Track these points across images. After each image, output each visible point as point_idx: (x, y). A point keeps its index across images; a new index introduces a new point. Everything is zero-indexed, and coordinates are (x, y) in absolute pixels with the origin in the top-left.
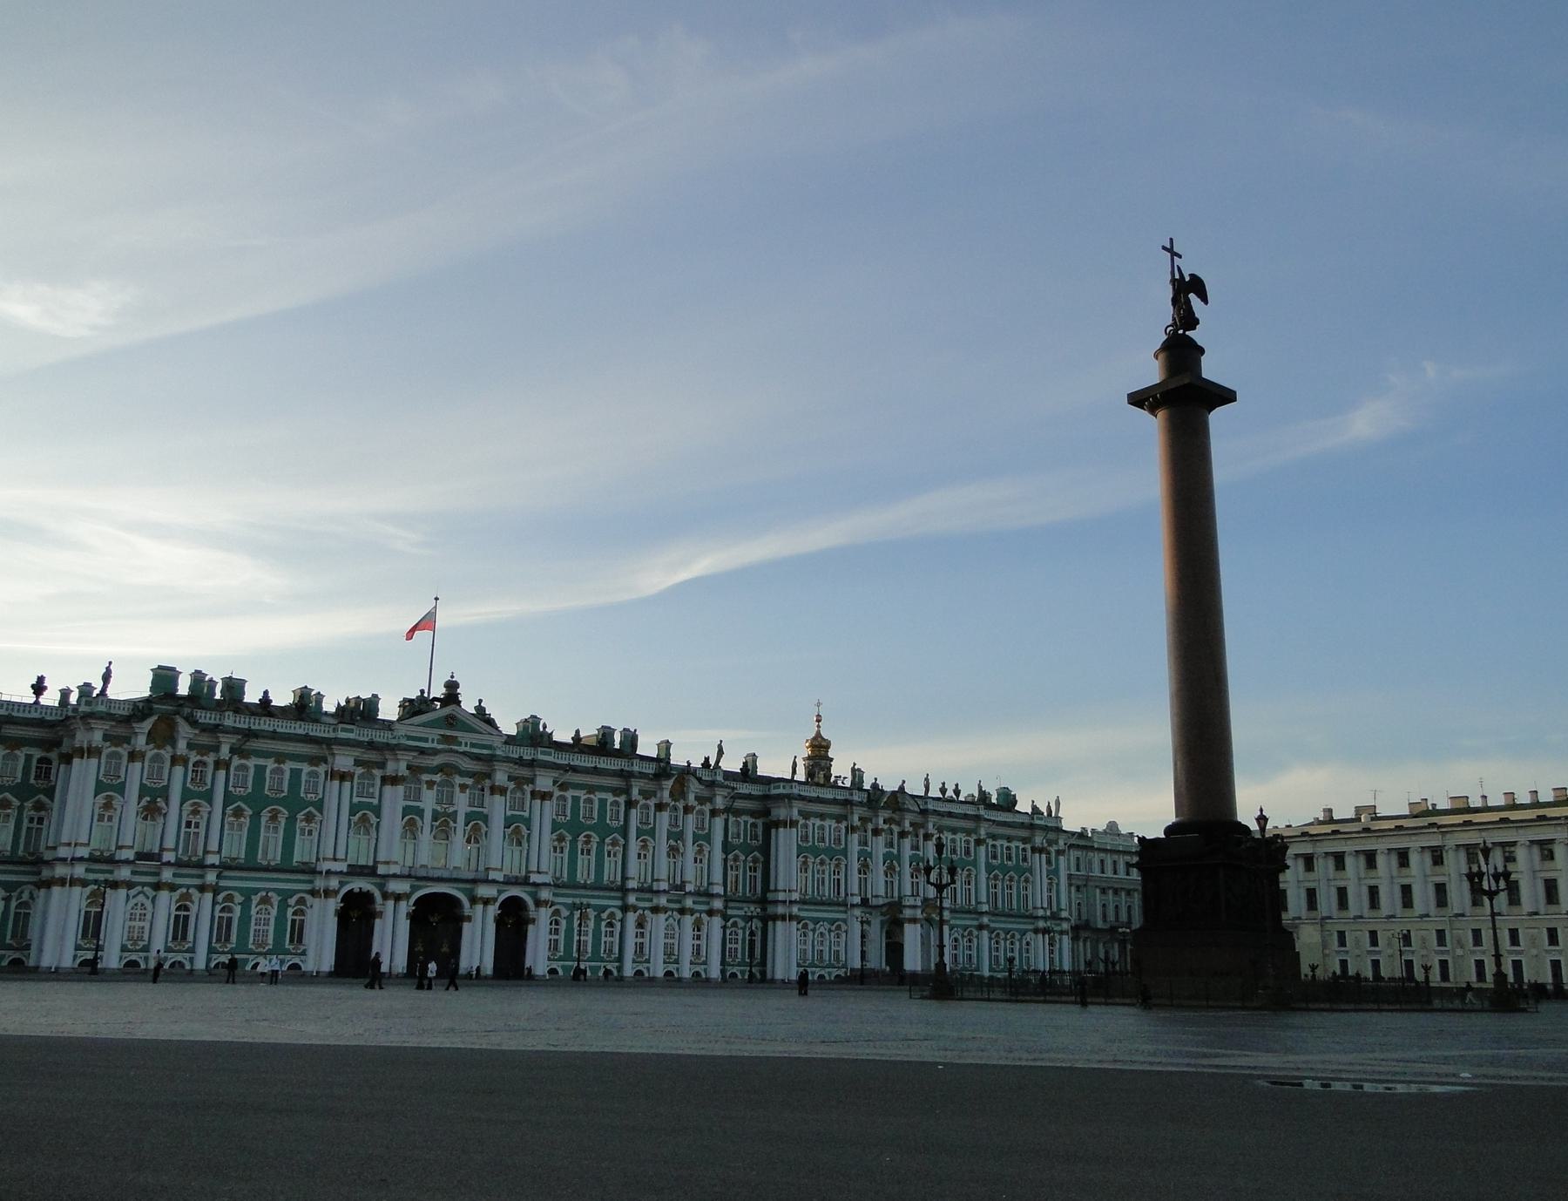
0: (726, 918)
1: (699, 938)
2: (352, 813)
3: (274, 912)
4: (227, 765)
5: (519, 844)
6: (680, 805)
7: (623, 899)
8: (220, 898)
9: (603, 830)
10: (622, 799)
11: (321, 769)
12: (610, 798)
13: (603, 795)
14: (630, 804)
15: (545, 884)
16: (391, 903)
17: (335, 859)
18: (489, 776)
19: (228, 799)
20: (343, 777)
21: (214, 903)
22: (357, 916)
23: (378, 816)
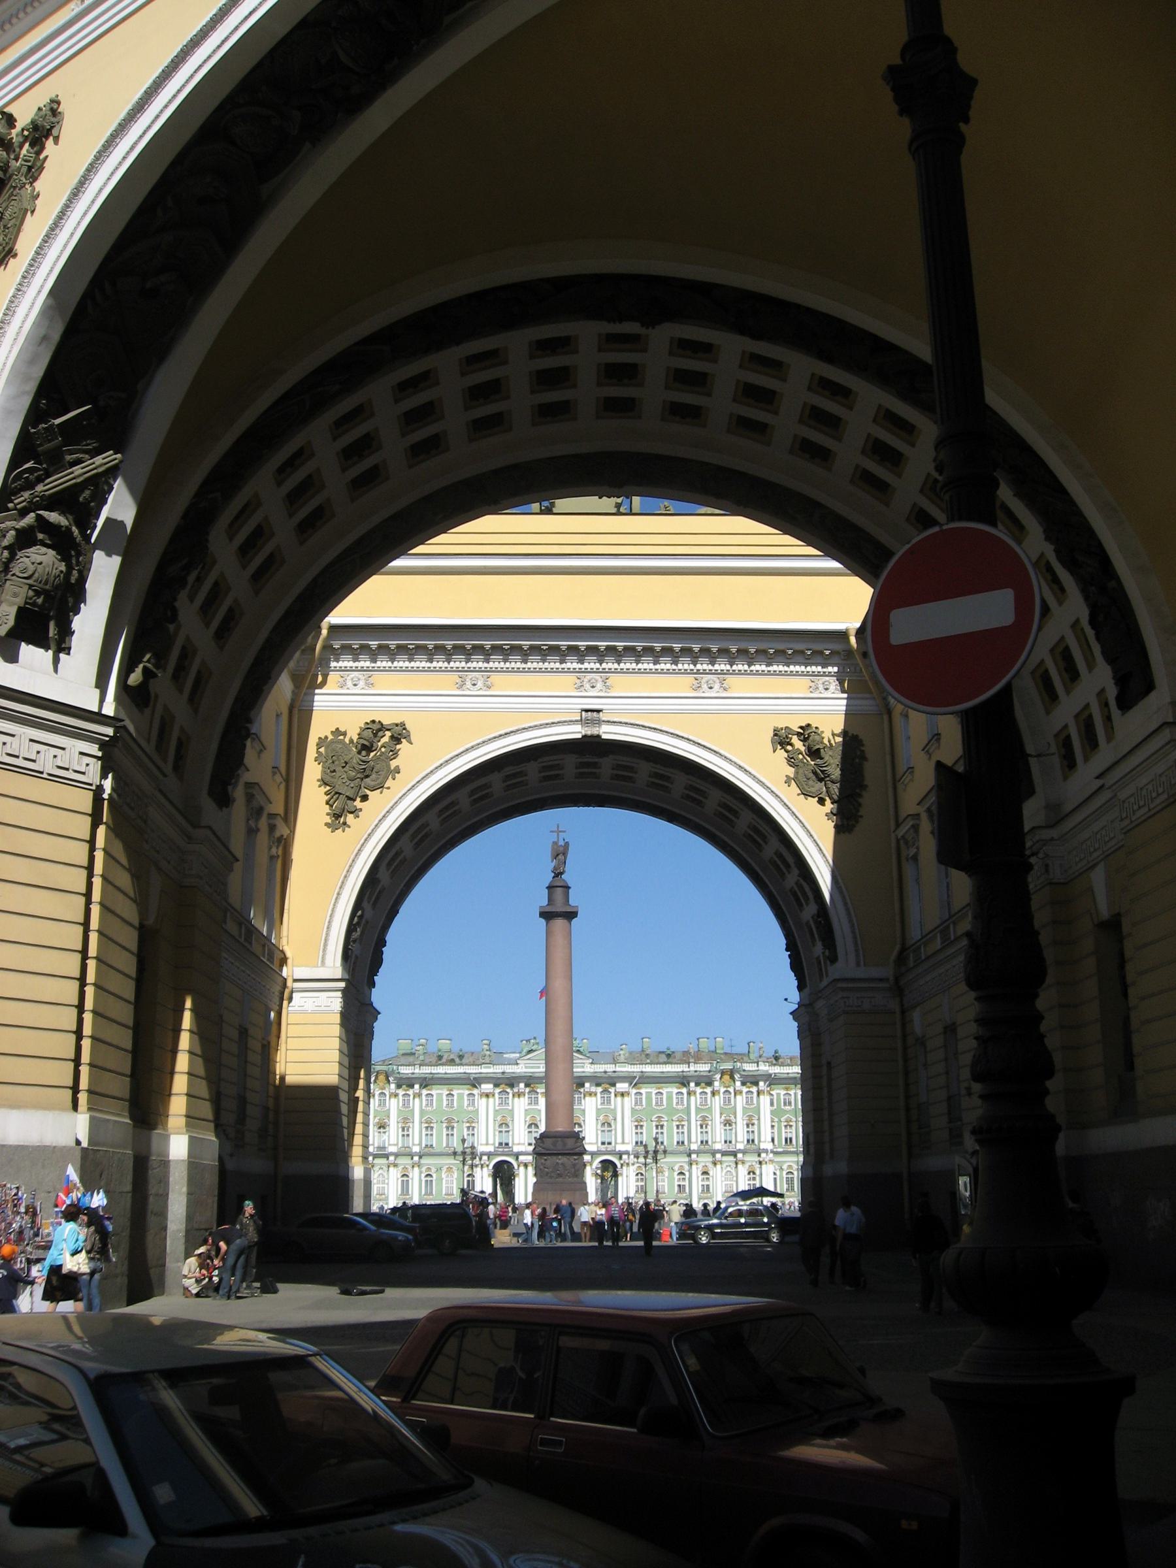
0: (780, 1164)
1: (754, 1179)
2: (495, 1117)
3: (455, 1176)
4: (420, 1095)
5: (609, 1125)
6: (731, 1090)
7: (689, 1155)
8: (424, 1169)
9: (671, 1111)
10: (684, 1090)
11: (475, 1092)
12: (675, 1091)
13: (669, 1090)
14: (689, 1094)
15: (627, 1153)
16: (522, 1168)
17: (487, 1144)
18: (583, 1085)
19: (422, 1112)
20: (487, 1096)
21: (421, 1173)
22: (504, 1174)
23: (513, 1117)
